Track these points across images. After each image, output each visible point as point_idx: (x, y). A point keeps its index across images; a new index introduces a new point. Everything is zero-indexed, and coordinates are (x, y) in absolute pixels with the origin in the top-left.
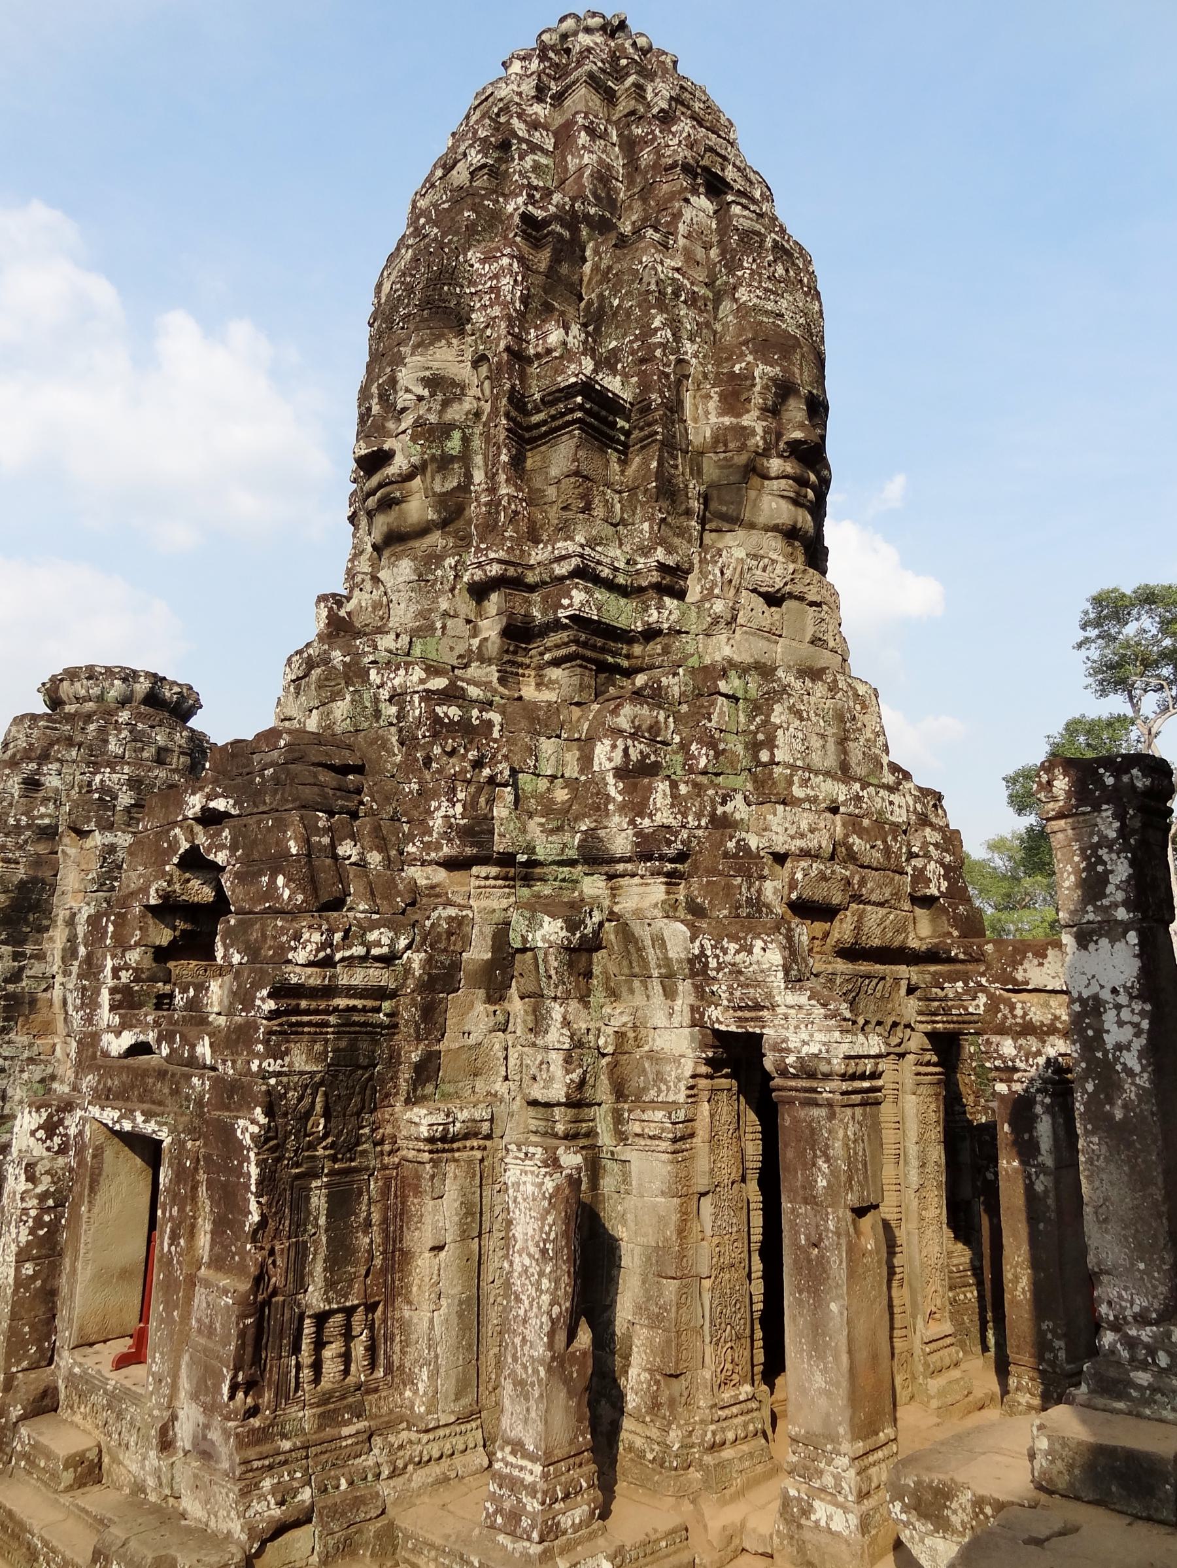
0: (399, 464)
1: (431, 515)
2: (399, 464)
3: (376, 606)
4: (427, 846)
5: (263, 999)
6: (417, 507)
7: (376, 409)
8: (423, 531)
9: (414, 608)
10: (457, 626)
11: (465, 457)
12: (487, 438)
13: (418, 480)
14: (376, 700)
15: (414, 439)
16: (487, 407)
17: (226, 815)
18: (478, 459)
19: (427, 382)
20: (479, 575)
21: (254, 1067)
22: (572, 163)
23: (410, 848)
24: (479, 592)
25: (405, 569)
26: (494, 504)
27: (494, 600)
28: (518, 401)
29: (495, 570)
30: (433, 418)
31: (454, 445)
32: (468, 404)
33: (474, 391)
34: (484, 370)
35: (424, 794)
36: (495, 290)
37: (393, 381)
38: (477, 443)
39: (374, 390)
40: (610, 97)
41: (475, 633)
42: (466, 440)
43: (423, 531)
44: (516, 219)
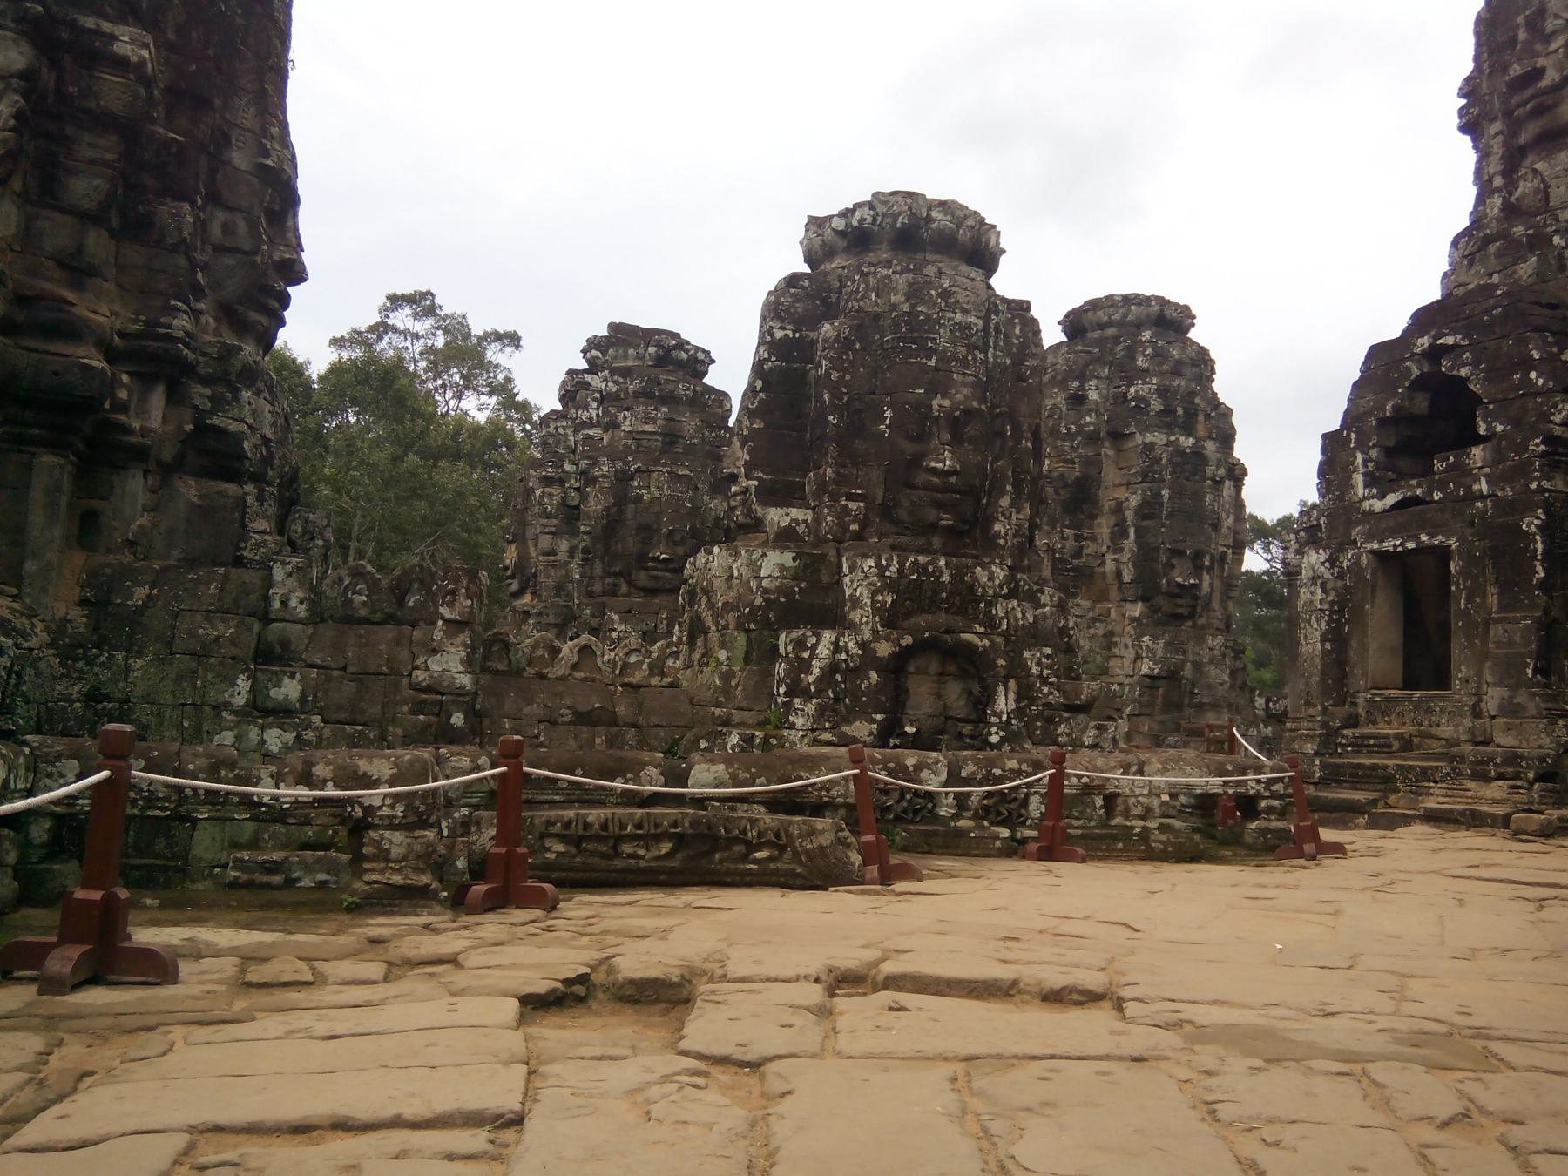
3: (1536, 191)
5: (1537, 445)
17: (1455, 346)
21: (1534, 485)
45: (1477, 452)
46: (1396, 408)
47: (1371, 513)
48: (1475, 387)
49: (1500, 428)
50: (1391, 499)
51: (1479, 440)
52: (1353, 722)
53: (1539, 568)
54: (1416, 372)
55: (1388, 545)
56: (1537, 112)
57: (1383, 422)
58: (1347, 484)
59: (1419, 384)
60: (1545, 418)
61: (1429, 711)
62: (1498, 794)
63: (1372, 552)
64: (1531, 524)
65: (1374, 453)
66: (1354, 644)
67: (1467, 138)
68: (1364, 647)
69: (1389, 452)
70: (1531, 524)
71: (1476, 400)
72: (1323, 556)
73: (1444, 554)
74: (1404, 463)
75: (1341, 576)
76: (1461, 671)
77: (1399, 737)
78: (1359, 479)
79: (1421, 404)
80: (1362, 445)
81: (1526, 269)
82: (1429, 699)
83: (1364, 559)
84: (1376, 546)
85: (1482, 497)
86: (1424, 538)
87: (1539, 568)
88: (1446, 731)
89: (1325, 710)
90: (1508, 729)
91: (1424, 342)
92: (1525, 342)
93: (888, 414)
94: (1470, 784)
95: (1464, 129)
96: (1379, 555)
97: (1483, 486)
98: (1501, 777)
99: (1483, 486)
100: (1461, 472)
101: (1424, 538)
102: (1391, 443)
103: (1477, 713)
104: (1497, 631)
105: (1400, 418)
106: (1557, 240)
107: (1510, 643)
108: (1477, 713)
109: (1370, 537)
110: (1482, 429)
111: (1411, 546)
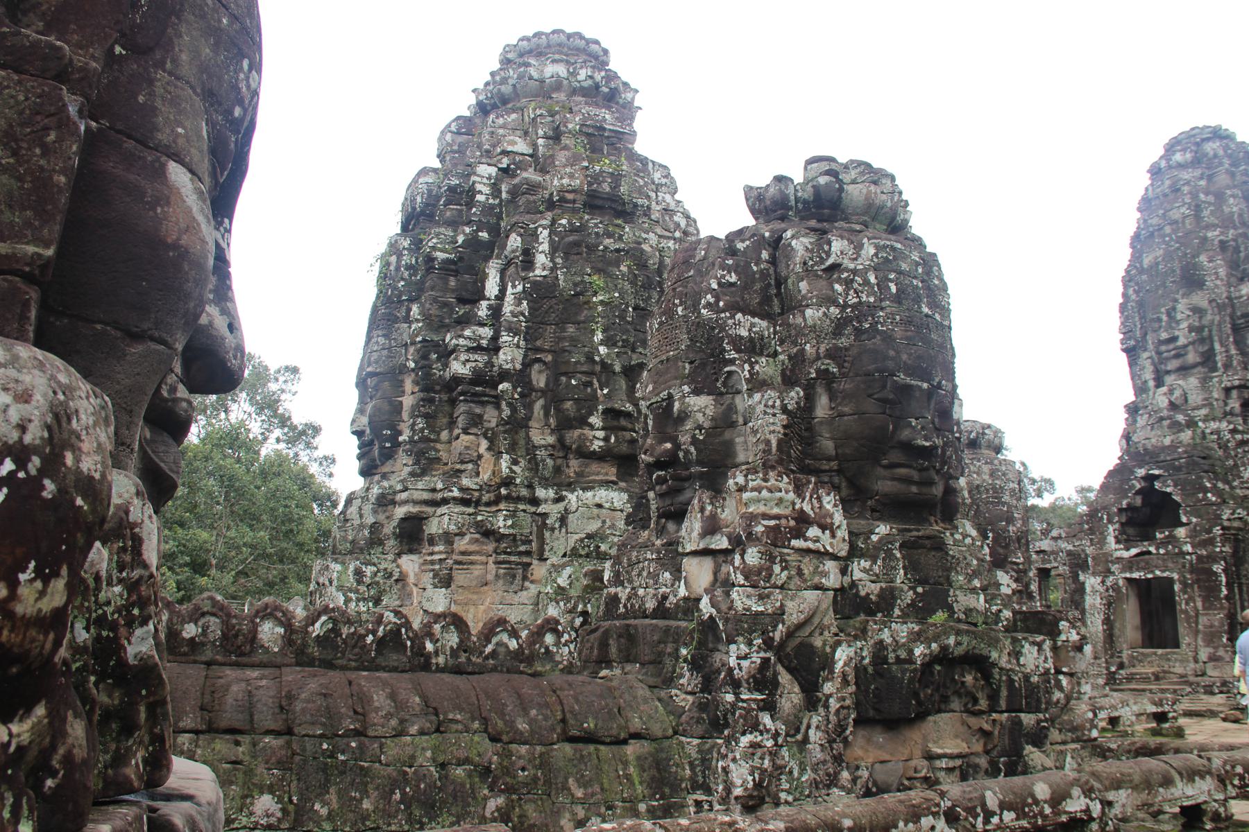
0: (1182, 341)
1: (1198, 360)
2: (1182, 341)
4: (1242, 483)
6: (1192, 357)
7: (1164, 318)
8: (1194, 366)
9: (1201, 397)
10: (1221, 403)
11: (1210, 337)
12: (1220, 330)
13: (1190, 348)
14: (1203, 432)
15: (1190, 332)
16: (1217, 318)
18: (1216, 338)
19: (1191, 310)
20: (1229, 384)
22: (1226, 210)
23: (1235, 484)
24: (1228, 390)
25: (1193, 382)
26: (1229, 357)
27: (1234, 393)
28: (1232, 316)
29: (1237, 383)
30: (1197, 324)
31: (1206, 333)
32: (1209, 317)
33: (1210, 312)
34: (1214, 304)
35: (1236, 465)
36: (1216, 273)
37: (1174, 309)
38: (1214, 332)
39: (1163, 310)
40: (1233, 175)
41: (1226, 404)
42: (1210, 331)
43: (1194, 366)
44: (1216, 242)
45: (1181, 532)
46: (1128, 504)
47: (1119, 559)
48: (1177, 498)
49: (1194, 520)
50: (1134, 551)
51: (1182, 525)
52: (1121, 666)
53: (1224, 589)
54: (1138, 486)
55: (1136, 575)
56: (1177, 356)
57: (1121, 510)
58: (1102, 542)
59: (1138, 493)
60: (1219, 517)
61: (1169, 660)
62: (1221, 701)
63: (1126, 578)
64: (1218, 568)
65: (1117, 526)
66: (1117, 625)
67: (1124, 355)
68: (1124, 627)
69: (1122, 524)
70: (1218, 568)
71: (1179, 505)
72: (1099, 579)
73: (1170, 581)
74: (1131, 531)
75: (1107, 590)
76: (1185, 640)
77: (1153, 674)
78: (1111, 540)
79: (1138, 501)
80: (1110, 521)
81: (1186, 436)
82: (1167, 654)
83: (1121, 582)
84: (1128, 575)
85: (1189, 554)
86: (1158, 573)
87: (1224, 589)
88: (1179, 670)
89: (1107, 662)
90: (1215, 668)
91: (1141, 472)
92: (1202, 478)
93: (990, 535)
94: (1203, 697)
95: (1123, 350)
96: (1129, 580)
97: (1188, 548)
98: (1221, 692)
99: (1188, 548)
100: (1172, 539)
101: (1158, 573)
102: (1124, 520)
103: (1196, 661)
104: (1203, 620)
105: (1130, 508)
106: (1200, 424)
107: (1211, 626)
108: (1196, 661)
109: (1123, 570)
110: (1184, 519)
111: (1150, 576)
